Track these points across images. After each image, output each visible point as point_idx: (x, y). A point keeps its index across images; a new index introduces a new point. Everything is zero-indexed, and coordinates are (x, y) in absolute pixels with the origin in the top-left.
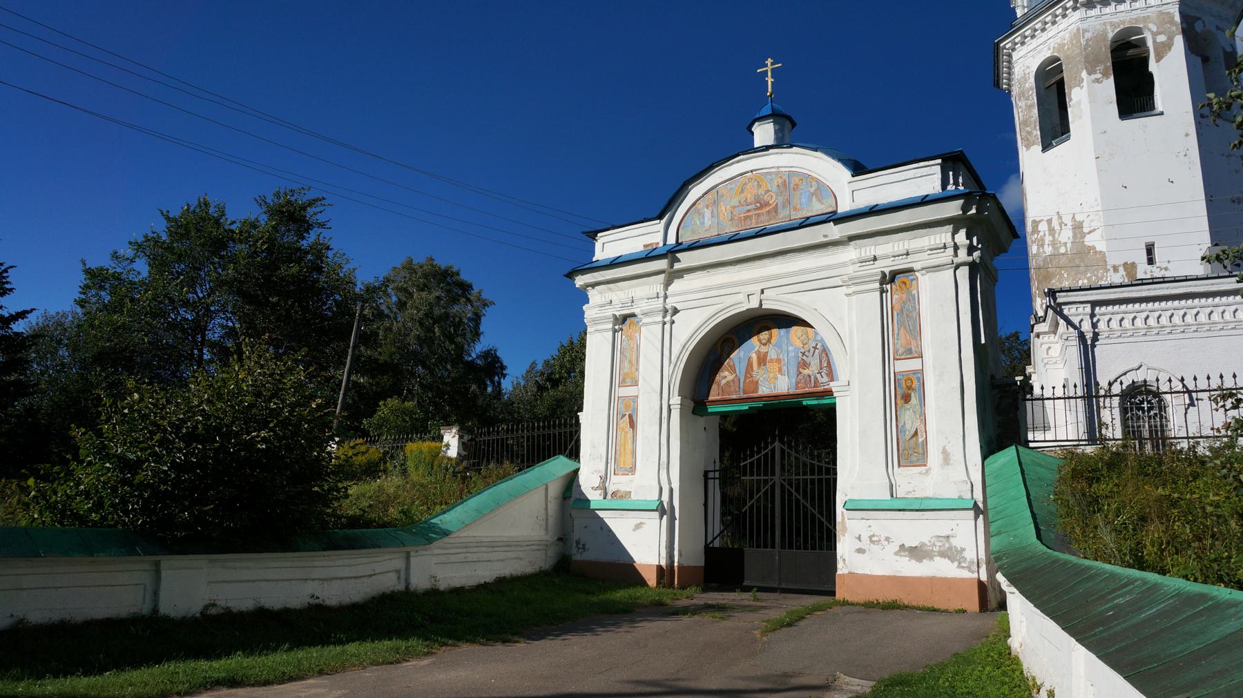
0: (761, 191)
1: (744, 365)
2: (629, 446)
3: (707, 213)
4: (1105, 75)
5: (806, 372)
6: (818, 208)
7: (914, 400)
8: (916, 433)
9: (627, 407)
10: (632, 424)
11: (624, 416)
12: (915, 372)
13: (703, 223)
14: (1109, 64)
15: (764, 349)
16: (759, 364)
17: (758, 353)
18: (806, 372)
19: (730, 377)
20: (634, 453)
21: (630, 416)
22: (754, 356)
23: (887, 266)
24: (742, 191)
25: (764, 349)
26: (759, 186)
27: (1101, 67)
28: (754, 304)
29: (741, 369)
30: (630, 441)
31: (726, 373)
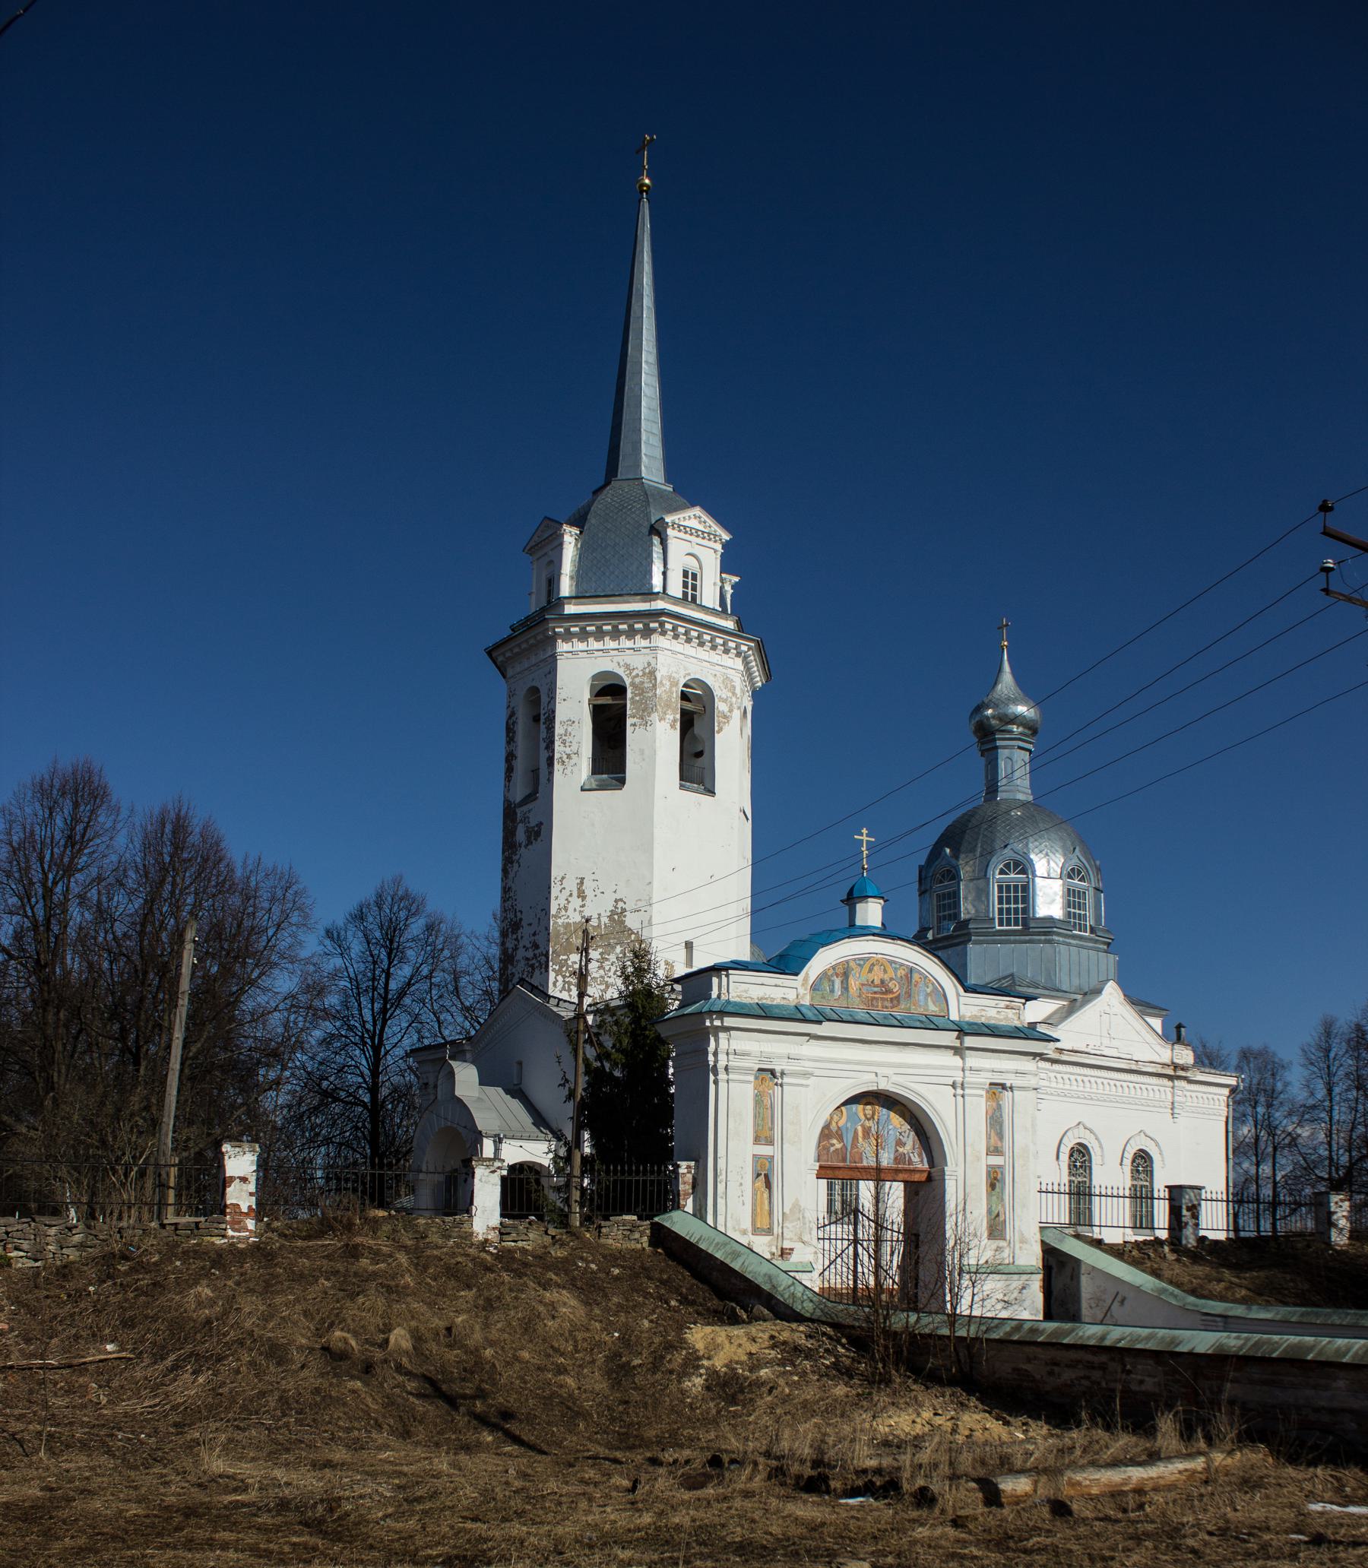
0: (886, 977)
1: (851, 1135)
2: (767, 1207)
3: (838, 982)
4: (673, 727)
5: (901, 1150)
6: (933, 1008)
7: (997, 1189)
8: (998, 1215)
9: (762, 1166)
10: (768, 1185)
11: (759, 1175)
12: (1000, 1167)
13: (832, 991)
14: (678, 716)
15: (868, 1124)
16: (864, 1138)
17: (863, 1126)
18: (901, 1150)
19: (838, 1146)
20: (771, 1213)
21: (766, 1176)
22: (859, 1128)
23: (986, 1079)
24: (870, 971)
25: (868, 1124)
26: (885, 971)
27: (670, 717)
28: (884, 1085)
29: (848, 1139)
30: (766, 1202)
31: (834, 1141)
